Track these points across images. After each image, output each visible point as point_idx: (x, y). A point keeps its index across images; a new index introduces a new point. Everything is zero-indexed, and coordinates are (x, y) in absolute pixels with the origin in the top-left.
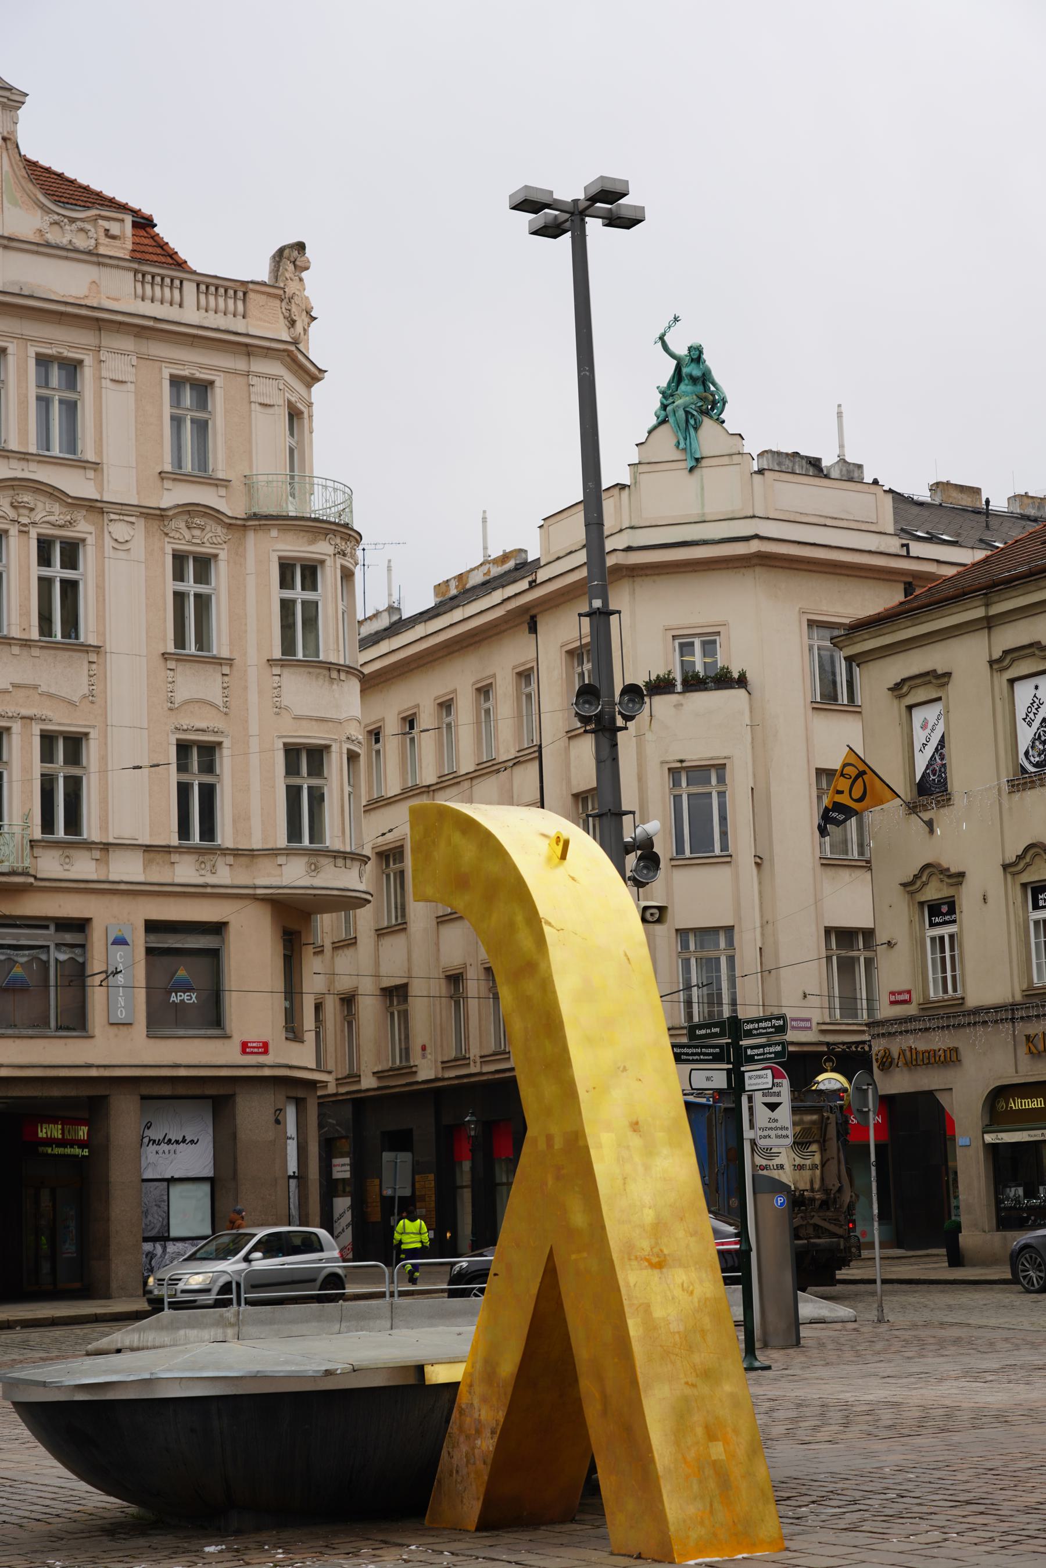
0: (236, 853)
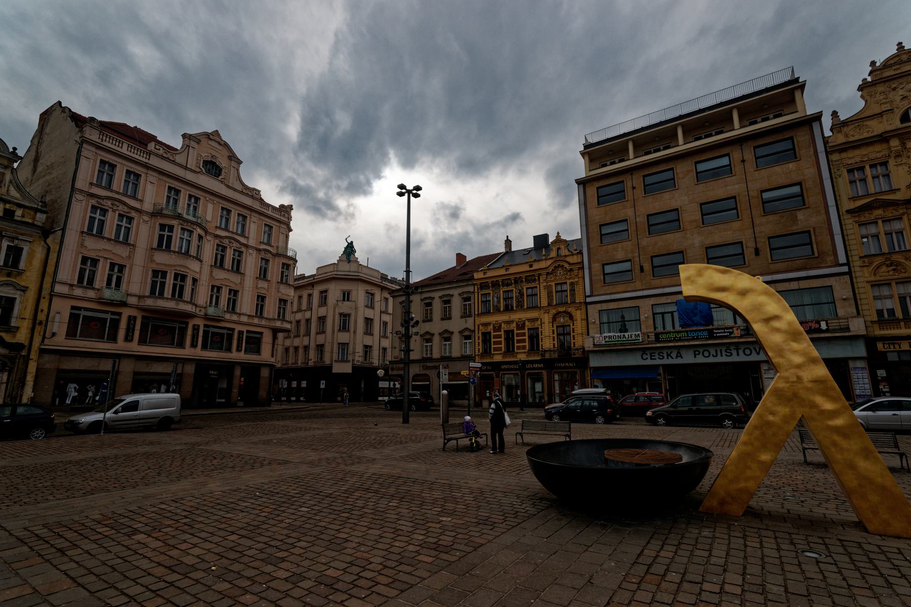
0: (267, 319)
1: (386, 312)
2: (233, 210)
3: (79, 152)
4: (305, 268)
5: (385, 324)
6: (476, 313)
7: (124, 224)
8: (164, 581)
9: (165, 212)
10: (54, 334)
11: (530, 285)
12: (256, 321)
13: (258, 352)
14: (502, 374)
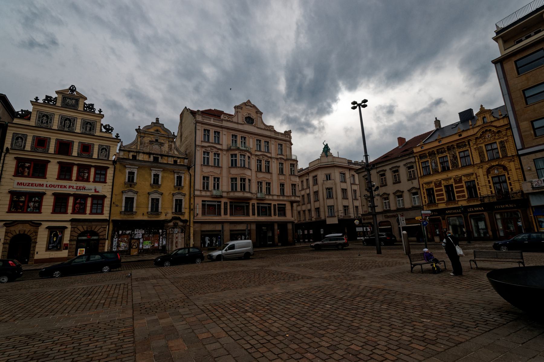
0: (286, 196)
1: (354, 184)
2: (262, 140)
3: (196, 127)
4: (303, 164)
6: (419, 176)
7: (216, 158)
9: (232, 148)
10: (197, 214)
11: (461, 150)
12: (281, 198)
13: (284, 215)
14: (447, 217)
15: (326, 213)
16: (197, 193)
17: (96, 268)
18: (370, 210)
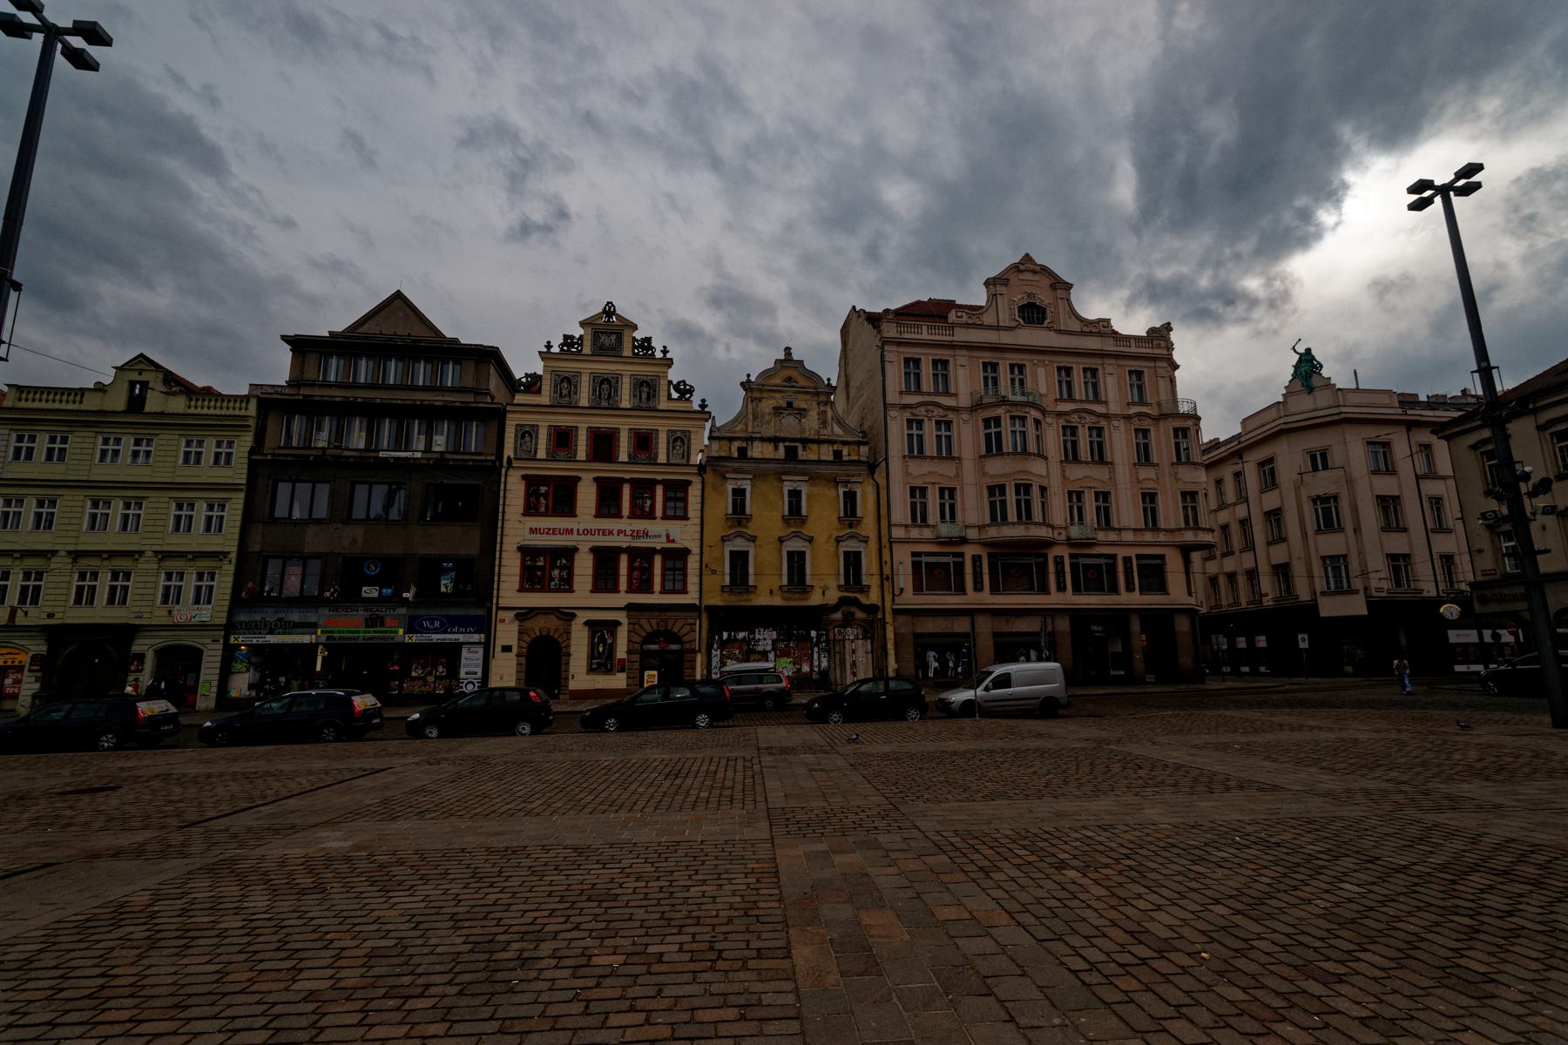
0: (1166, 530)
1: (1432, 475)
2: (1074, 366)
3: (882, 356)
4: (1217, 426)
5: (1437, 502)
7: (943, 433)
8: (1129, 952)
9: (986, 401)
10: (902, 590)
12: (1148, 537)
13: (1162, 588)
15: (1317, 581)
16: (898, 533)
17: (675, 717)
18: (1509, 566)
